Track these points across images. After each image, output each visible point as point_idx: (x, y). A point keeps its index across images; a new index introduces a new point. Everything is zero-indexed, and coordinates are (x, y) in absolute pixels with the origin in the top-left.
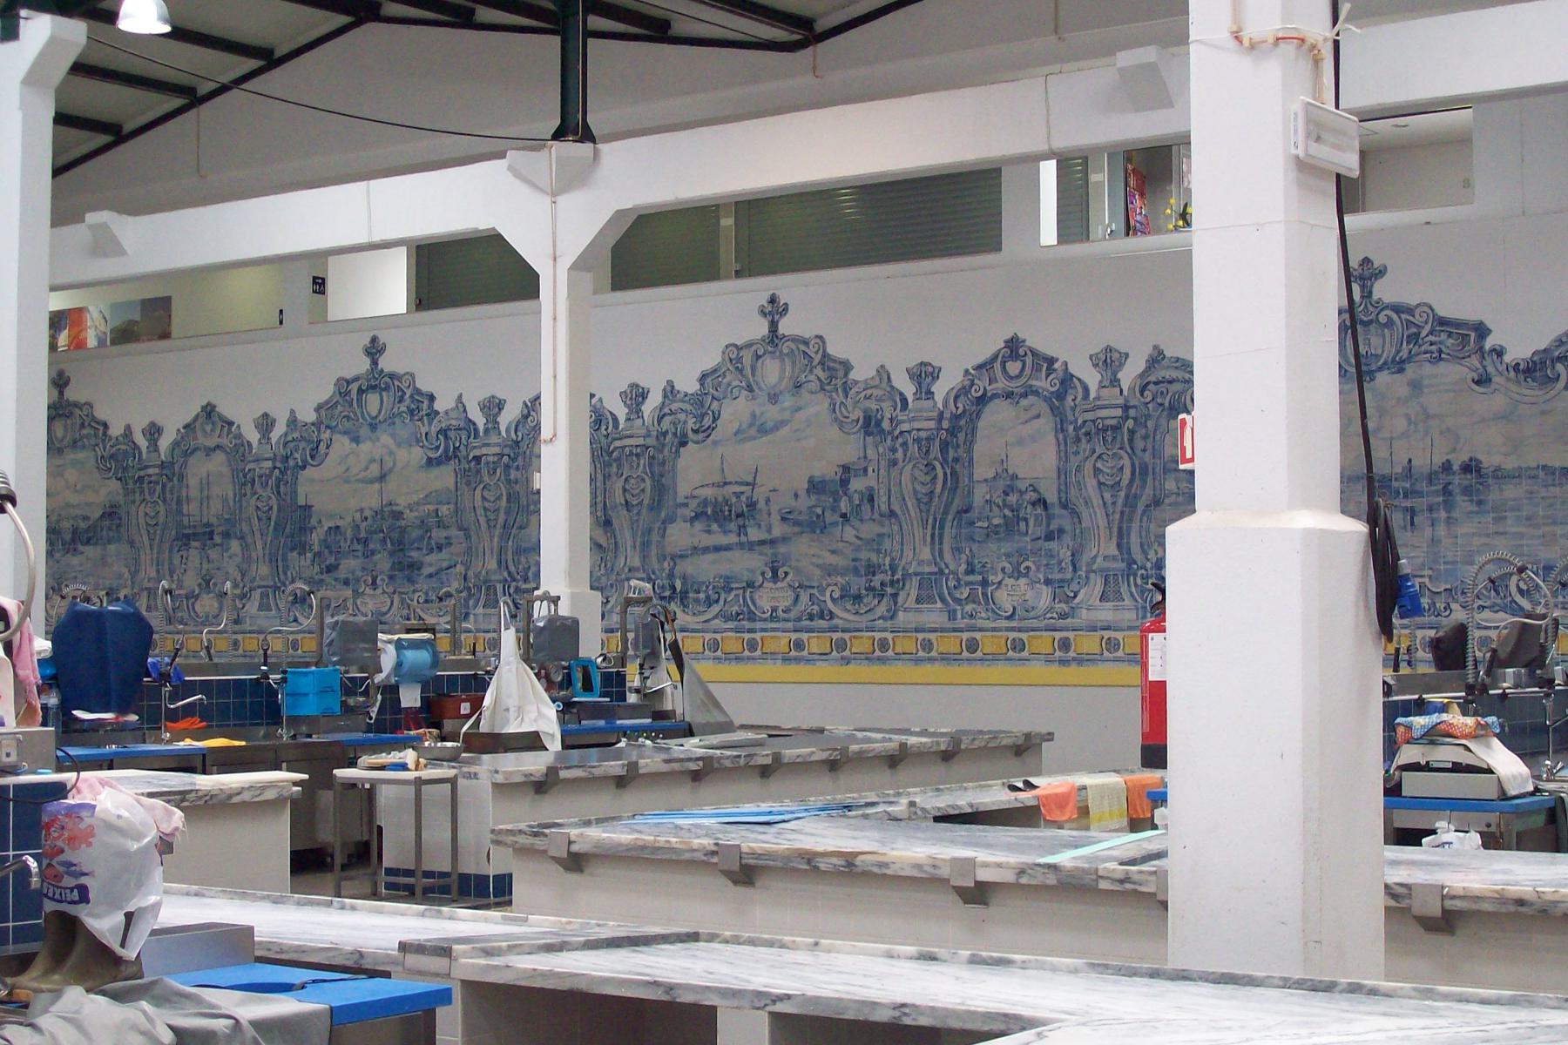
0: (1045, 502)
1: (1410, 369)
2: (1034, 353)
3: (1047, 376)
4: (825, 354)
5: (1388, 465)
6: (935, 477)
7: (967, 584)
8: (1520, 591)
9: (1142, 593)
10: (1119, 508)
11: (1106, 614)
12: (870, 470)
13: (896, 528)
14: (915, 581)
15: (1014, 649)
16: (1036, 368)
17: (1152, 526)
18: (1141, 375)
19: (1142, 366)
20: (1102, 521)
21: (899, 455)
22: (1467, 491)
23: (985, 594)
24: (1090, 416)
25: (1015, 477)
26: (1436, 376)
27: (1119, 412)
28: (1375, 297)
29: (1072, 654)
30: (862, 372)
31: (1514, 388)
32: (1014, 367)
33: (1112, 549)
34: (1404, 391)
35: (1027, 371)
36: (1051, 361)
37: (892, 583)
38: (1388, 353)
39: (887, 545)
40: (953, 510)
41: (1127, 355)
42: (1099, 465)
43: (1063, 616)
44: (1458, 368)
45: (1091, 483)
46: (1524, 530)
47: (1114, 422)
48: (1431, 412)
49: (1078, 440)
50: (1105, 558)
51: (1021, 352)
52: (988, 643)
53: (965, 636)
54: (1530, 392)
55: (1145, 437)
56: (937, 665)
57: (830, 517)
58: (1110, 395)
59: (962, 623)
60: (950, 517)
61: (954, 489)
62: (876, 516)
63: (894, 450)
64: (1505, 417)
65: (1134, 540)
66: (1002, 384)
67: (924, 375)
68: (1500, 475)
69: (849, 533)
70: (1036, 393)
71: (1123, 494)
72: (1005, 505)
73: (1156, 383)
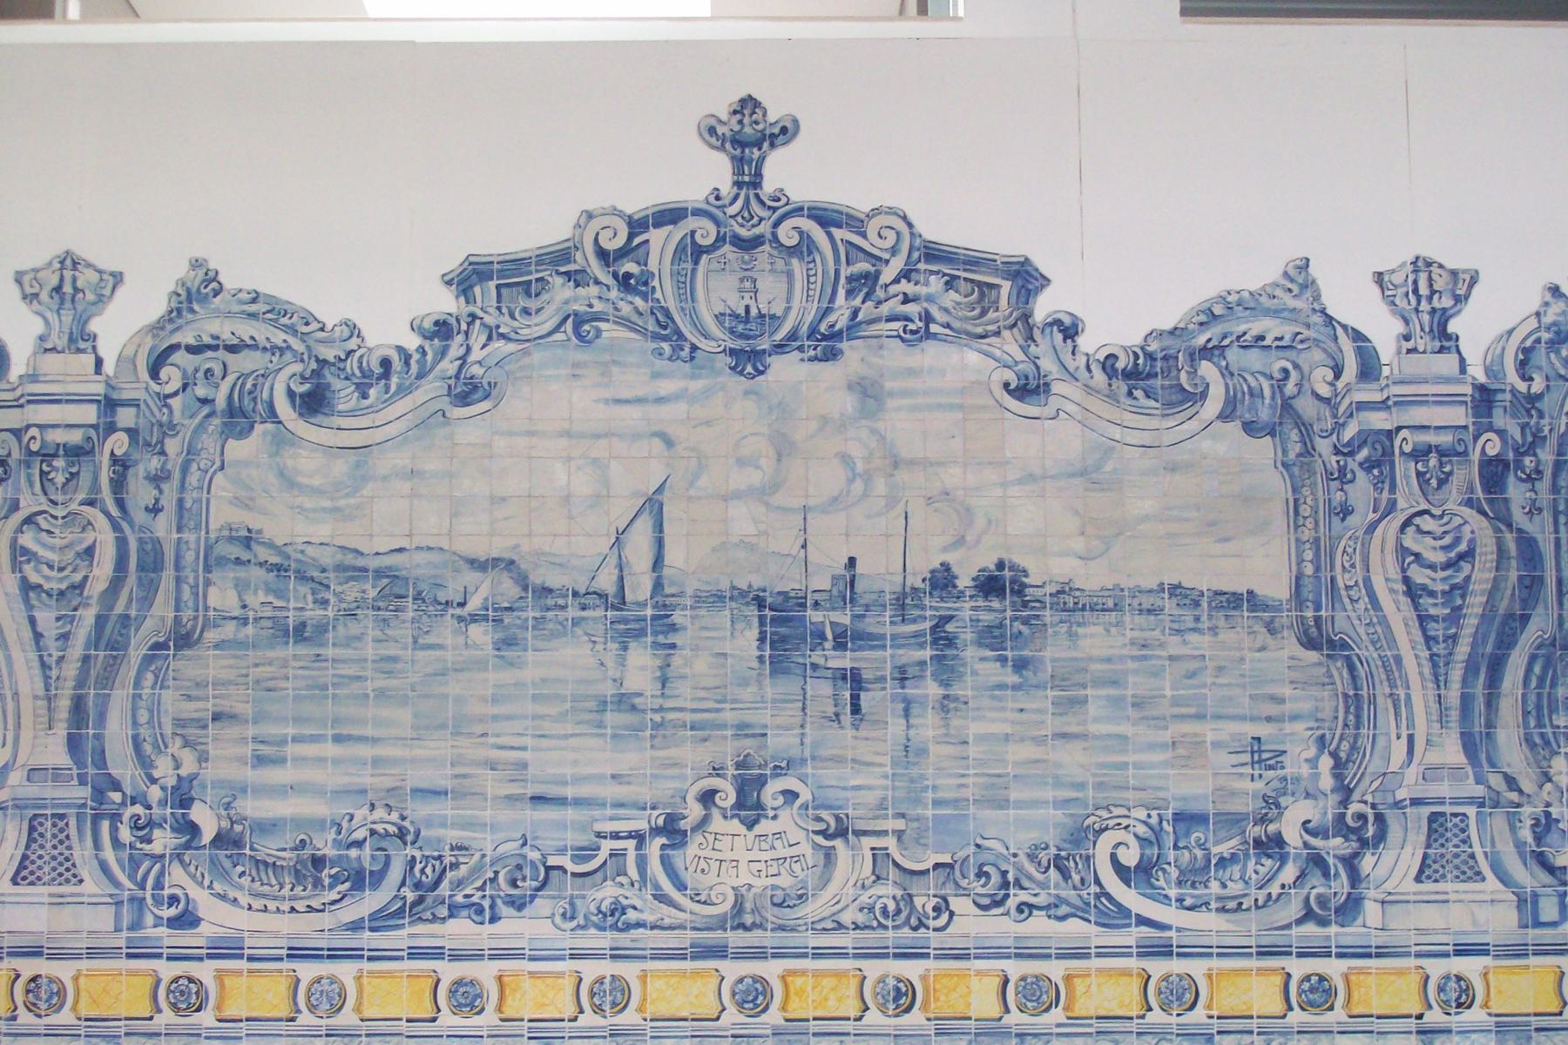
1: (852, 350)
5: (796, 572)
9: (135, 863)
10: (77, 650)
17: (168, 696)
18: (157, 328)
19: (157, 308)
22: (992, 637)
26: (911, 372)
27: (89, 414)
31: (1096, 405)
33: (57, 755)
34: (847, 403)
38: (801, 313)
41: (118, 278)
42: (27, 539)
44: (973, 357)
46: (1125, 729)
47: (75, 437)
48: (905, 453)
50: (33, 772)
54: (1135, 424)
55: (157, 479)
64: (1088, 474)
65: (116, 732)
68: (1073, 604)
71: (88, 616)
73: (194, 350)
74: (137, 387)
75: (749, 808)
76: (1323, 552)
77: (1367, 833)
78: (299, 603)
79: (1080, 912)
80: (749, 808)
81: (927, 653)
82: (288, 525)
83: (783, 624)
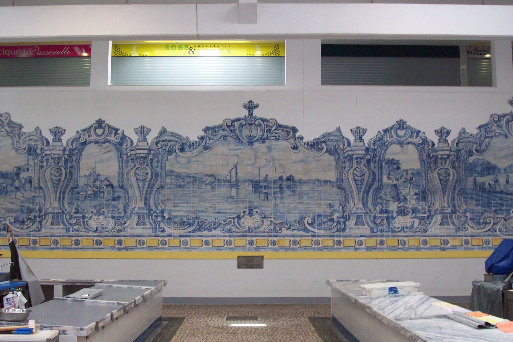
0: (112, 185)
1: (267, 142)
2: (109, 126)
3: (115, 136)
4: (10, 122)
6: (61, 174)
7: (75, 217)
8: (308, 224)
10: (145, 189)
11: (139, 230)
12: (30, 169)
13: (42, 194)
14: (51, 216)
15: (97, 244)
16: (110, 133)
18: (157, 138)
19: (157, 135)
20: (138, 194)
21: (45, 164)
22: (289, 187)
23: (83, 222)
24: (134, 152)
25: (99, 175)
26: (277, 145)
27: (146, 152)
28: (254, 115)
29: (123, 246)
30: (28, 129)
32: (99, 131)
34: (266, 150)
35: (106, 133)
36: (117, 130)
37: (39, 217)
38: (259, 135)
39: (37, 200)
40: (70, 187)
41: (150, 130)
42: (137, 172)
43: (119, 231)
45: (133, 180)
47: (144, 155)
49: (128, 161)
50: (139, 208)
51: (103, 125)
52: (85, 242)
53: (74, 239)
54: (312, 153)
55: (158, 162)
56: (60, 250)
57: (9, 188)
58: (143, 145)
59: (71, 233)
60: (68, 190)
61: (70, 179)
62: (32, 189)
63: (42, 162)
65: (152, 202)
66: (94, 138)
67: (58, 133)
68: (301, 182)
69: (19, 195)
70: (109, 142)
71: (147, 183)
72: (94, 186)
73: (163, 141)
74: (154, 147)
75: (251, 214)
76: (341, 174)
77: (347, 218)
78: (180, 182)
79: (302, 230)
80: (251, 214)
81: (279, 190)
82: (177, 169)
83: (256, 185)
